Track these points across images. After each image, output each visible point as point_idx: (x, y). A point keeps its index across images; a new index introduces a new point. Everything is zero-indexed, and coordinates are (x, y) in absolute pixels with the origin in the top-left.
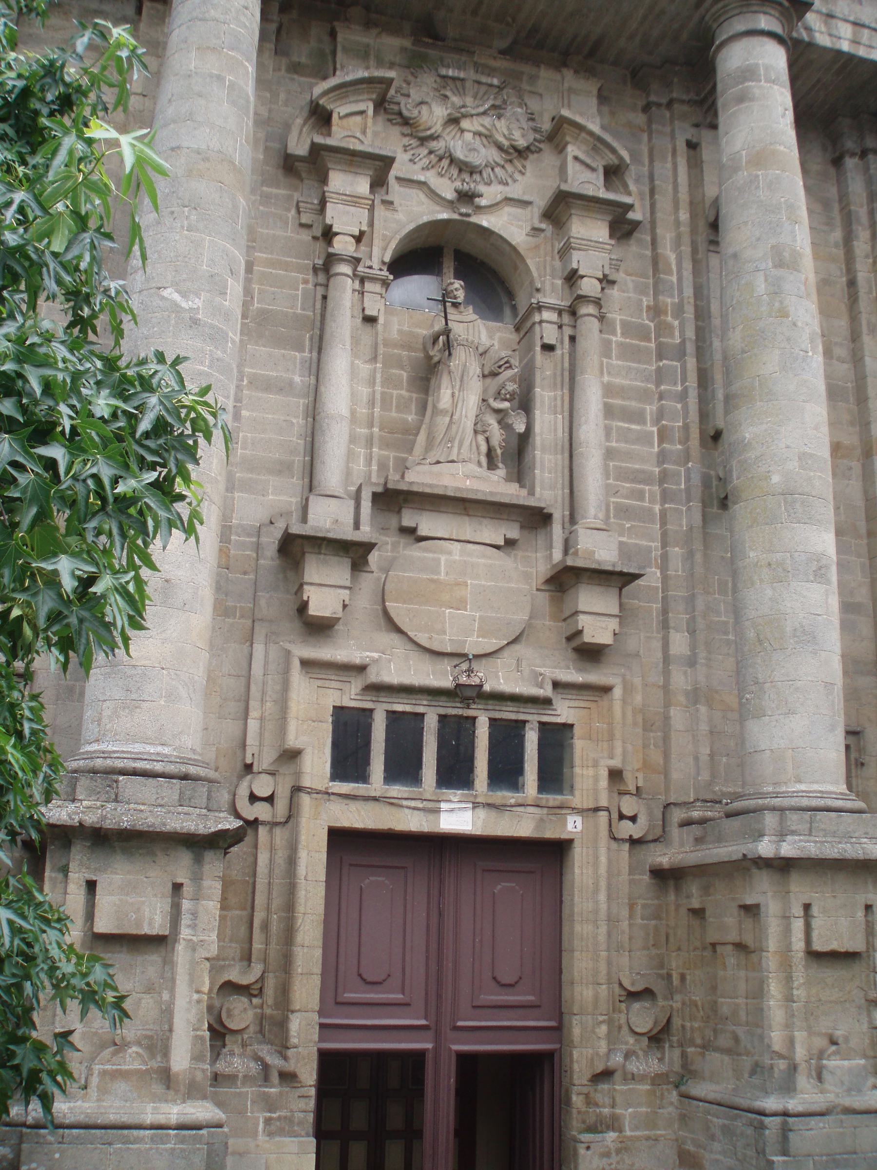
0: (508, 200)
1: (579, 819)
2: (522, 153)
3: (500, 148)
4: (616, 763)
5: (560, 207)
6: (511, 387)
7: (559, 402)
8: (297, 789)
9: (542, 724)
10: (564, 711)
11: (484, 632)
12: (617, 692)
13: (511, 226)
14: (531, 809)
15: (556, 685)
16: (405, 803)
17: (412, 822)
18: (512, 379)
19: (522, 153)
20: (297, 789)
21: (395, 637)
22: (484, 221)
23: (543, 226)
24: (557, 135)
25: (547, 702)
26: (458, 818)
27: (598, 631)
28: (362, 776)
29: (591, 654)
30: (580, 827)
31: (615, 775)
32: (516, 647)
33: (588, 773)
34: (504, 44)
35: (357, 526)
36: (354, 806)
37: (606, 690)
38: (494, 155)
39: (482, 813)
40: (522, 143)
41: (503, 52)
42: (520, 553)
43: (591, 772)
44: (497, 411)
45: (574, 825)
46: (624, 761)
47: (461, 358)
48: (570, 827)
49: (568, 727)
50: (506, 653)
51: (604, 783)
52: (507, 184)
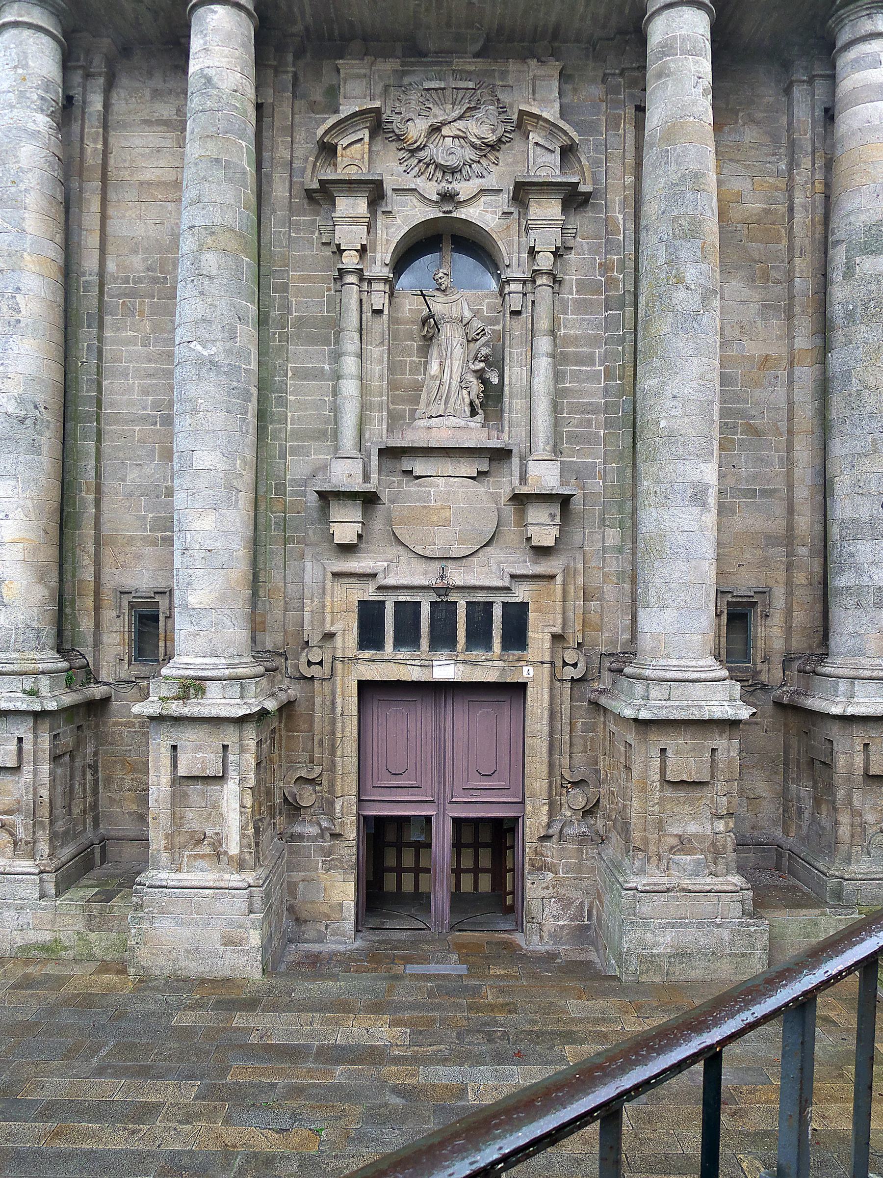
0: (483, 191)
1: (531, 669)
2: (493, 147)
3: (474, 146)
4: (558, 630)
5: (523, 193)
6: (485, 351)
7: (524, 357)
8: (334, 658)
9: (505, 604)
10: (521, 593)
11: (462, 541)
12: (559, 579)
13: (484, 215)
14: (496, 663)
15: (513, 576)
16: (408, 662)
17: (414, 674)
18: (486, 344)
19: (493, 147)
20: (334, 658)
21: (400, 548)
22: (462, 213)
23: (512, 209)
24: (524, 123)
25: (508, 589)
26: (444, 671)
27: (546, 537)
28: (379, 645)
29: (542, 552)
30: (532, 674)
31: (557, 638)
32: (488, 549)
33: (539, 637)
34: (477, 47)
35: (366, 478)
36: (374, 666)
37: (553, 577)
38: (470, 154)
39: (461, 667)
40: (492, 138)
41: (477, 55)
42: (491, 479)
43: (540, 636)
44: (475, 371)
45: (527, 673)
46: (563, 628)
47: (446, 330)
48: (525, 674)
49: (524, 605)
50: (480, 554)
51: (547, 645)
52: (483, 177)
